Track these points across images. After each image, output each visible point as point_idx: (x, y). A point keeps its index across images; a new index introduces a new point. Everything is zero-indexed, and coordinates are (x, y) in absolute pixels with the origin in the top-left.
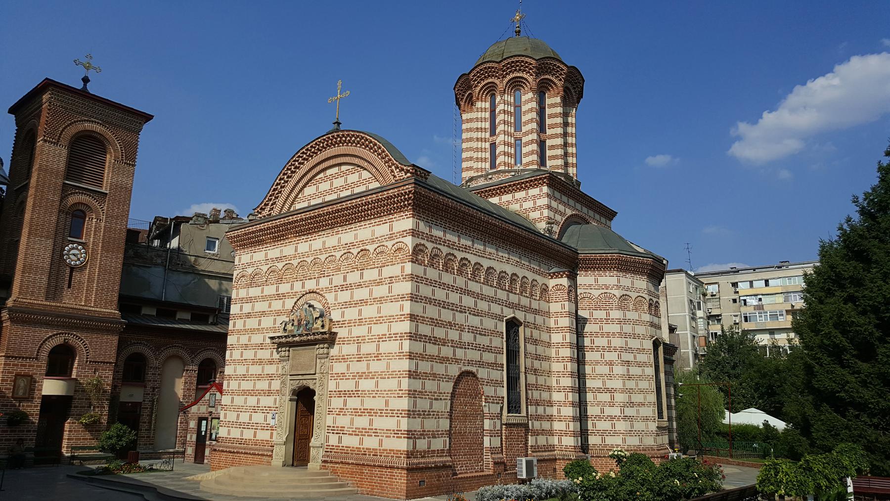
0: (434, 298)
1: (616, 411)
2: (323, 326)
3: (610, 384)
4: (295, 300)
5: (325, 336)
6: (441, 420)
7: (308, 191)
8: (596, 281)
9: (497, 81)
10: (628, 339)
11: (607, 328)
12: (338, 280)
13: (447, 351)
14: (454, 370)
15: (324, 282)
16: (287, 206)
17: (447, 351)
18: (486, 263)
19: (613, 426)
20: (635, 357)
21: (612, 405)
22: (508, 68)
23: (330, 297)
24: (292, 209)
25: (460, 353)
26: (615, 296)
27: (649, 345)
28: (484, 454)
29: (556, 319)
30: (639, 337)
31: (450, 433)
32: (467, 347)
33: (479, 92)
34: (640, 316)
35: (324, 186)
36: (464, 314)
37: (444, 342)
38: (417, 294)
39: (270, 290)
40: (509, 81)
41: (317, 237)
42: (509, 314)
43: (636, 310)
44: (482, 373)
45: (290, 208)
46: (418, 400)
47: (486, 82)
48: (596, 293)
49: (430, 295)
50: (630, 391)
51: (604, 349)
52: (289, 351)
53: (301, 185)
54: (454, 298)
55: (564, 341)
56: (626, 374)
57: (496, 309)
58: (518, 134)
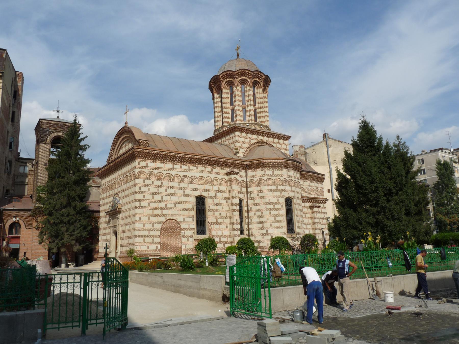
1: (264, 231)
3: (262, 220)
4: (113, 197)
6: (154, 239)
8: (256, 173)
10: (271, 199)
11: (261, 195)
13: (158, 212)
14: (163, 219)
15: (119, 189)
17: (158, 212)
18: (182, 174)
19: (263, 238)
20: (274, 206)
21: (262, 229)
23: (120, 195)
25: (166, 212)
26: (263, 179)
27: (283, 200)
28: (182, 251)
30: (276, 197)
31: (160, 243)
32: (170, 209)
34: (277, 187)
36: (169, 196)
37: (156, 208)
38: (140, 191)
39: (108, 194)
42: (197, 194)
43: (275, 185)
44: (180, 219)
46: (141, 231)
47: (217, 84)
48: (255, 179)
50: (272, 222)
51: (259, 204)
53: (118, 150)
54: (162, 190)
56: (269, 214)
57: (189, 192)
58: (232, 107)
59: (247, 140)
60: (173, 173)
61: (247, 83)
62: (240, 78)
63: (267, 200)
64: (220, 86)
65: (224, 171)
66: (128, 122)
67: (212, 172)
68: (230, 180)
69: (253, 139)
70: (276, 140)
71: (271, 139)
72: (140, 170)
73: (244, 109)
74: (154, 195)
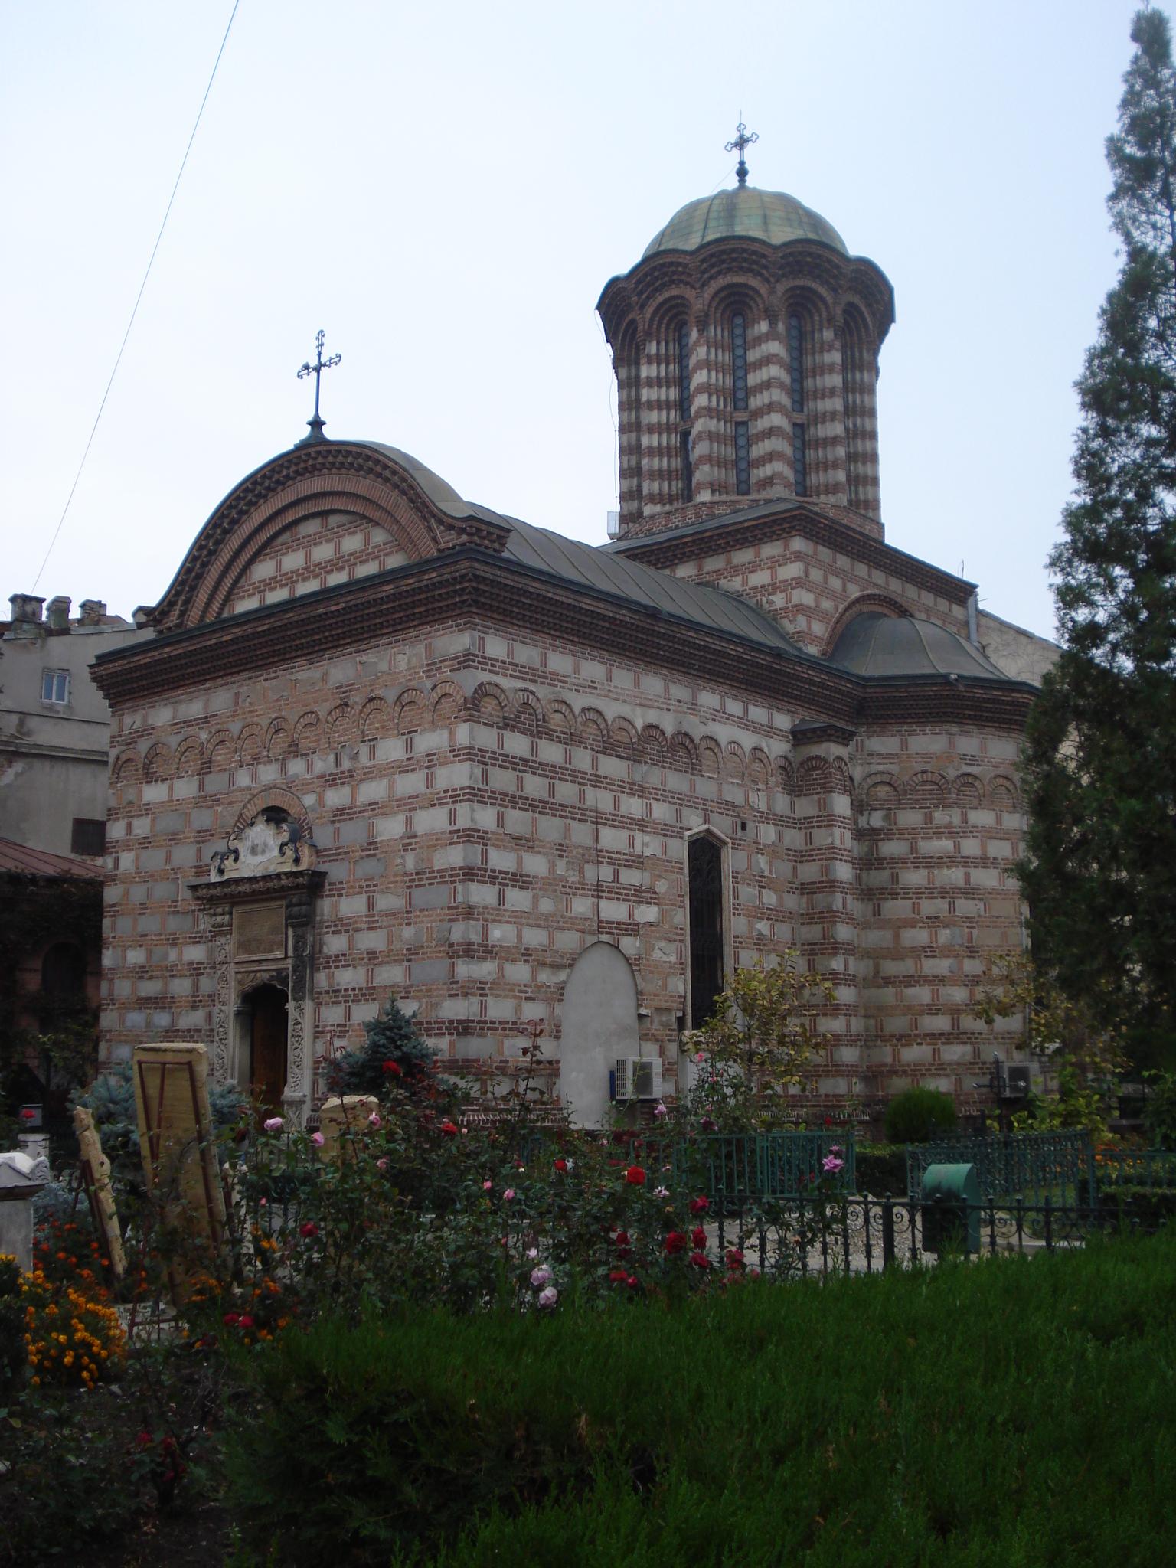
0: (522, 794)
2: (297, 861)
5: (300, 880)
7: (263, 570)
9: (689, 294)
12: (323, 764)
15: (296, 767)
16: (215, 607)
22: (713, 266)
24: (225, 615)
29: (808, 831)
33: (652, 320)
35: (293, 561)
40: (716, 294)
41: (279, 673)
42: (696, 825)
45: (222, 609)
46: (490, 1000)
47: (666, 295)
49: (511, 789)
51: (919, 894)
52: (231, 913)
54: (566, 791)
55: (824, 879)
59: (835, 583)
60: (612, 710)
61: (818, 311)
62: (791, 283)
63: (955, 876)
64: (677, 306)
65: (783, 721)
66: (323, 418)
67: (744, 723)
68: (817, 763)
69: (856, 580)
70: (928, 598)
71: (911, 591)
72: (484, 677)
73: (800, 428)
74: (537, 815)
